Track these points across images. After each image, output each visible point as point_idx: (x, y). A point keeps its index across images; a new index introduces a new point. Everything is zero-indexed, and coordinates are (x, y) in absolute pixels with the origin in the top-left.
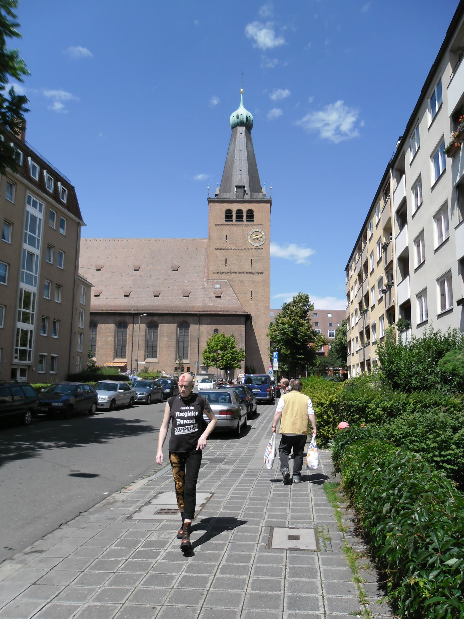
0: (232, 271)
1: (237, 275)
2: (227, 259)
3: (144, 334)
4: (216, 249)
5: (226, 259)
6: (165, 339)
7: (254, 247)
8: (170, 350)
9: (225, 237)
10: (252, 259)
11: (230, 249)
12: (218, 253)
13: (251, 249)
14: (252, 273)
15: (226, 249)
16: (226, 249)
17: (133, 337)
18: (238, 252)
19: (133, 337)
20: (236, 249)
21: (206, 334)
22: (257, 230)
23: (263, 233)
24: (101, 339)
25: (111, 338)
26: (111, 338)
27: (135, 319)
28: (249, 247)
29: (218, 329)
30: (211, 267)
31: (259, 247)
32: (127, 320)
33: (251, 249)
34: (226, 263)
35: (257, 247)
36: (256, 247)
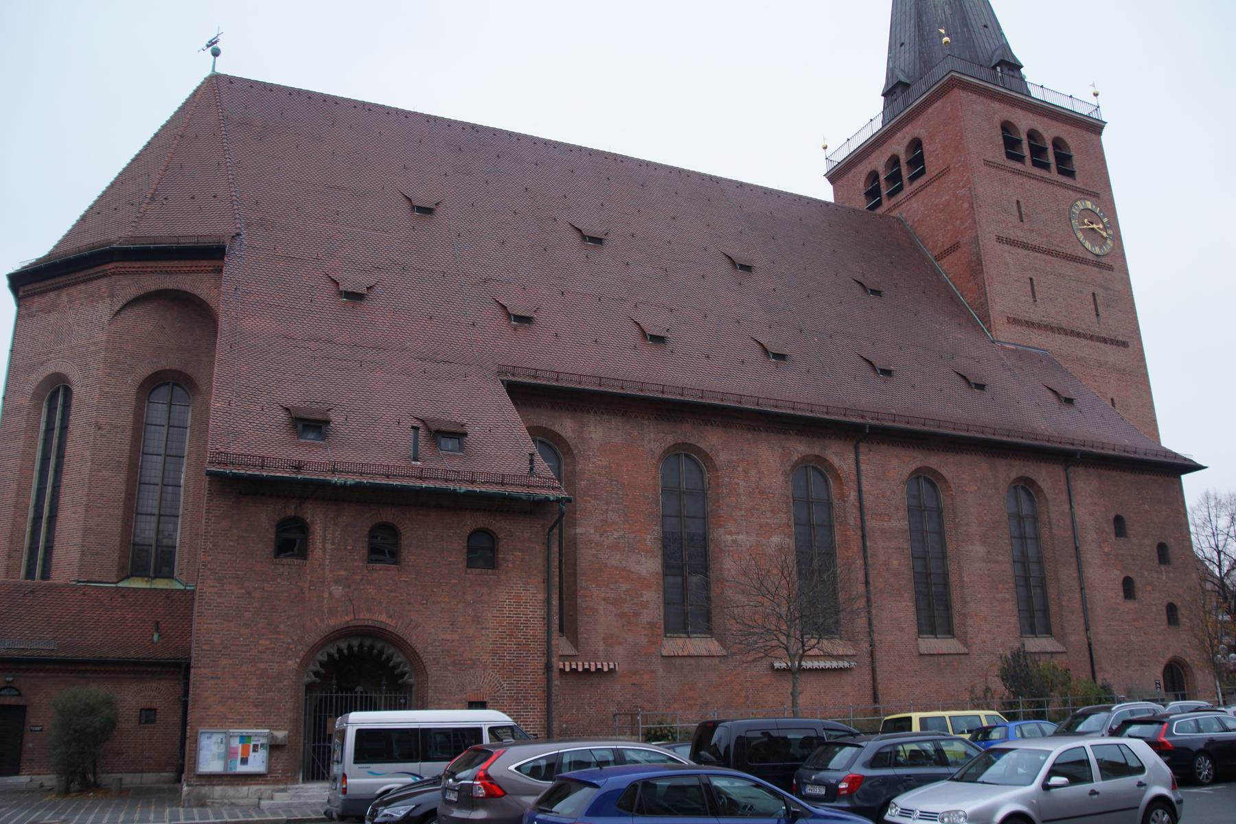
0: (1054, 323)
1: (1069, 338)
2: (1034, 278)
3: (904, 524)
4: (1000, 239)
5: (1031, 279)
6: (978, 549)
7: (1090, 257)
8: (999, 596)
9: (1015, 206)
10: (1094, 294)
11: (1034, 249)
12: (1007, 255)
13: (1083, 261)
14: (1104, 341)
15: (1025, 246)
16: (1025, 246)
17: (863, 537)
18: (1057, 263)
19: (863, 537)
20: (1049, 252)
21: (1095, 536)
22: (1089, 205)
23: (1105, 220)
24: (734, 541)
25: (776, 539)
26: (776, 539)
27: (861, 457)
28: (1080, 253)
29: (1124, 516)
30: (997, 300)
31: (1104, 260)
32: (835, 461)
33: (1083, 261)
34: (1034, 296)
35: (1099, 260)
36: (1095, 259)
